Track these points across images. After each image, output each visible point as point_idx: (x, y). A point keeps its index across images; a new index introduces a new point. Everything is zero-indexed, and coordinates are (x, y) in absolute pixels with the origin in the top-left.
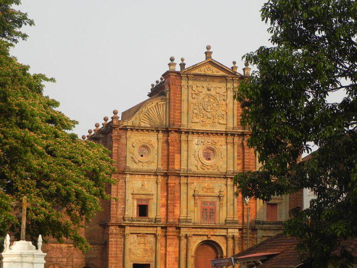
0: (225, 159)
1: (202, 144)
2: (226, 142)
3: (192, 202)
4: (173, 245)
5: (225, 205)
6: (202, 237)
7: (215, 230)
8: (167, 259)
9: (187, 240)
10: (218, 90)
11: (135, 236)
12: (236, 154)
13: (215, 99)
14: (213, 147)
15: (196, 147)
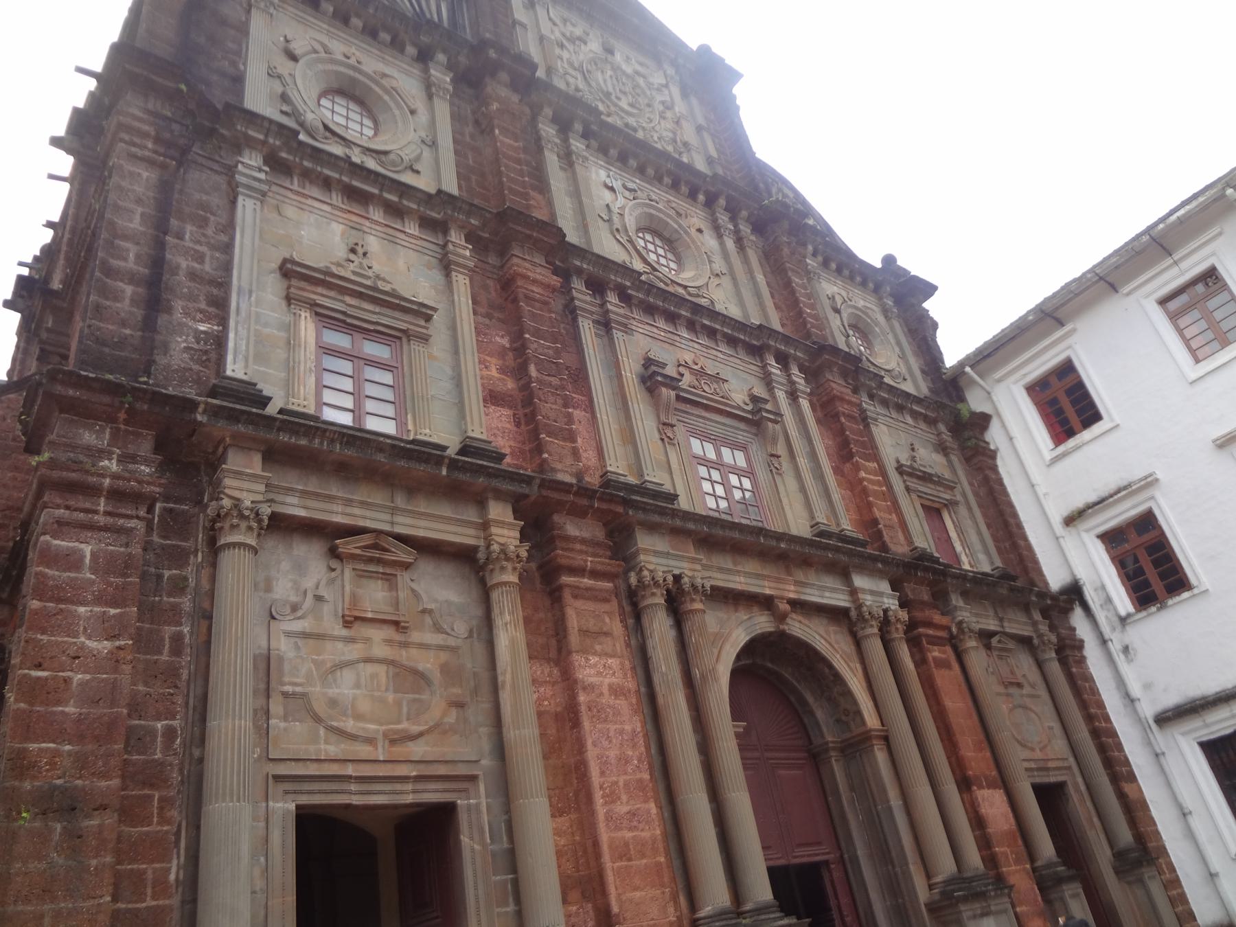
0: (726, 281)
1: (627, 193)
2: (717, 229)
3: (645, 423)
4: (606, 645)
5: (785, 465)
6: (743, 615)
7: (800, 575)
8: (591, 754)
9: (679, 624)
10: (639, 68)
11: (310, 553)
12: (760, 278)
13: (636, 86)
14: (676, 226)
15: (608, 196)
